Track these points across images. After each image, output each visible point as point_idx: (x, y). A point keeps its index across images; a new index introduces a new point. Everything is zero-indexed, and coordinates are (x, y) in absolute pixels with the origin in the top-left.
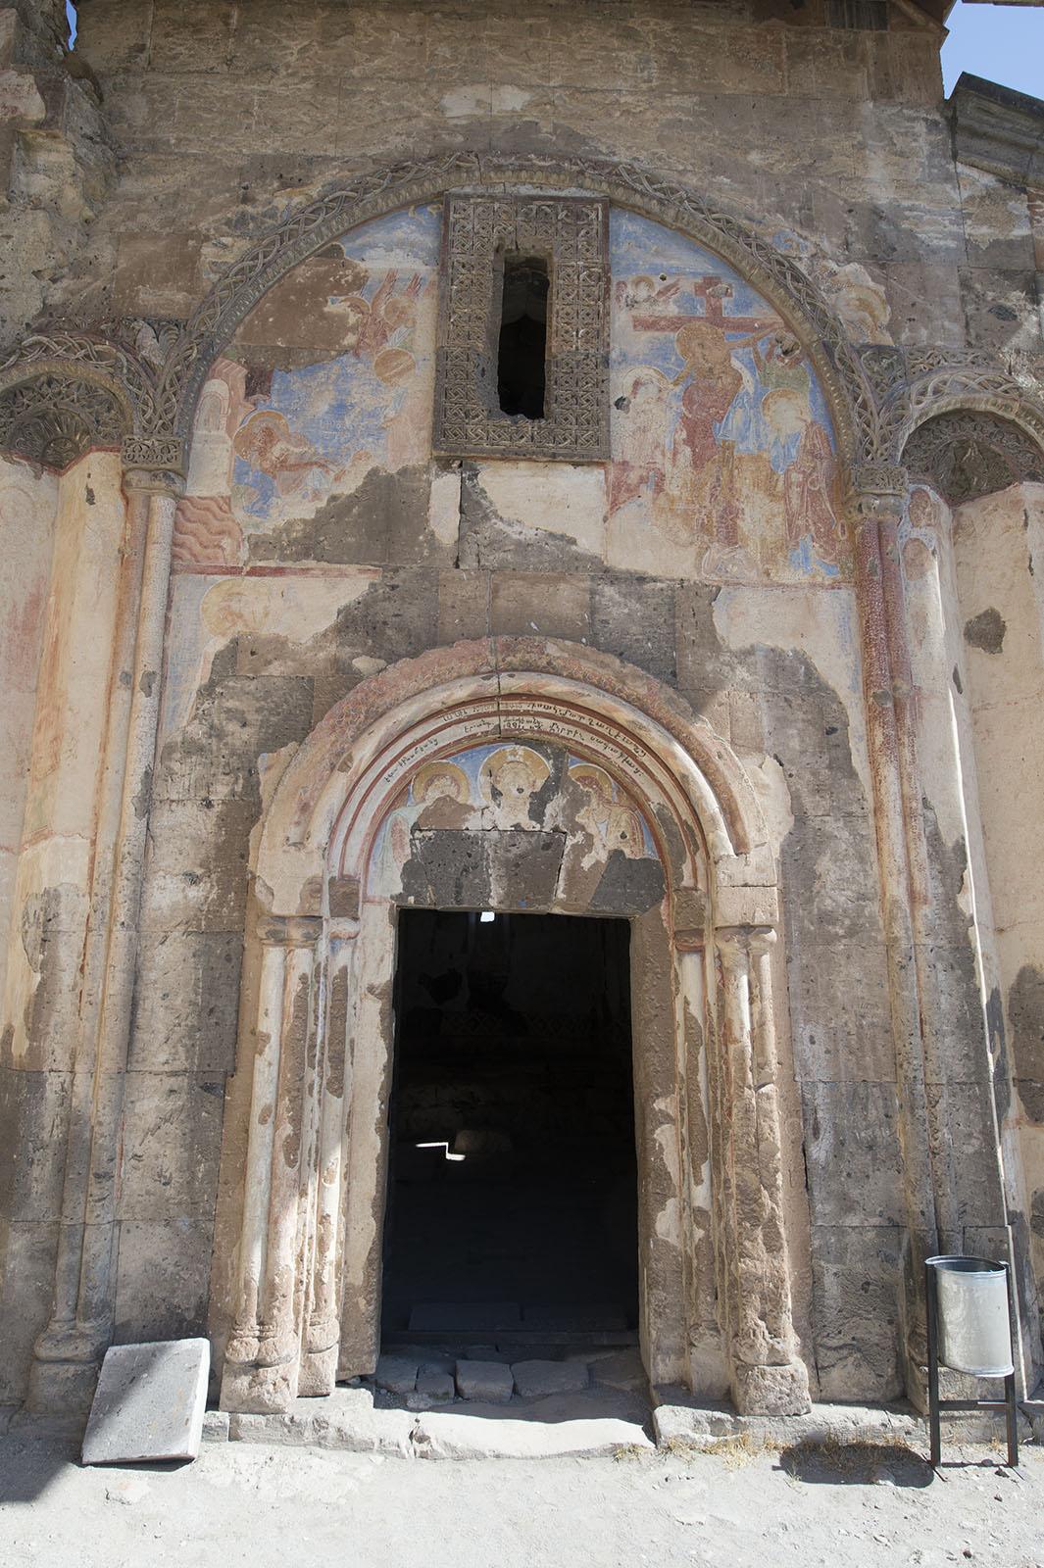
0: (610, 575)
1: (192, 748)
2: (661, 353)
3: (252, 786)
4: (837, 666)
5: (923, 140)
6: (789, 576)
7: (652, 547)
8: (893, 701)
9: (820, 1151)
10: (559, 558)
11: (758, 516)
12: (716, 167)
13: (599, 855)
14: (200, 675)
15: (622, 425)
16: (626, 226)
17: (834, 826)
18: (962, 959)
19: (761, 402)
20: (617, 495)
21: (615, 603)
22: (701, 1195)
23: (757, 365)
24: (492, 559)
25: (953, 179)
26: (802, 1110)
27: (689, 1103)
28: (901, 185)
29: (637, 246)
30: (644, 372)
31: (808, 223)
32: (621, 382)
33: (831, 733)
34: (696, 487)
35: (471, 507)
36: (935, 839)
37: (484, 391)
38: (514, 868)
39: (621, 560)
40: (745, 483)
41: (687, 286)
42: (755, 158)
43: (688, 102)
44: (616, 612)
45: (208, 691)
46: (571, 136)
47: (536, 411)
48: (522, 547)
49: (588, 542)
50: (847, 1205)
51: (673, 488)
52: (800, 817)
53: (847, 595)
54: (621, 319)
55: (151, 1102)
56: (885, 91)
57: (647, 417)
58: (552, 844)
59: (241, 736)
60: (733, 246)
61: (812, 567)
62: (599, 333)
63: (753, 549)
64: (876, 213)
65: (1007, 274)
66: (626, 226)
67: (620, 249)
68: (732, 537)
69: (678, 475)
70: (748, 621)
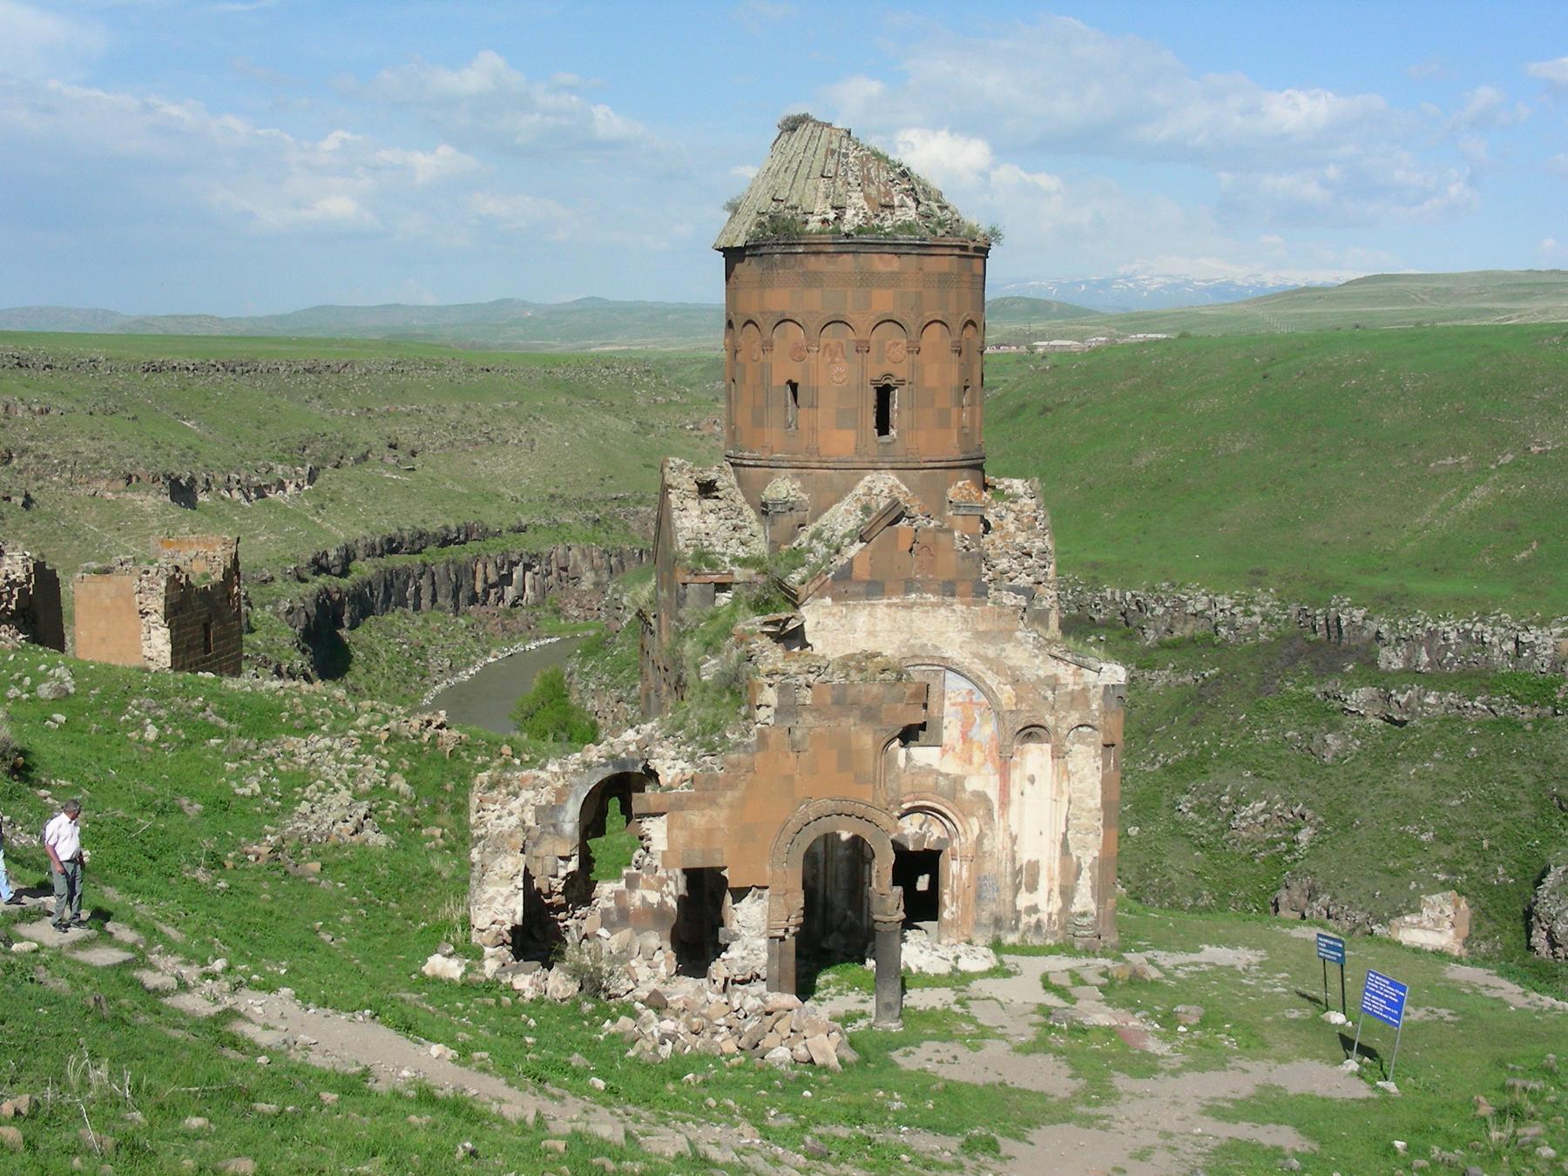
4: (993, 794)
6: (984, 771)
7: (951, 766)
10: (929, 770)
11: (977, 757)
15: (945, 733)
16: (949, 674)
18: (1014, 860)
19: (981, 726)
20: (944, 753)
21: (942, 781)
29: (952, 681)
33: (990, 811)
35: (908, 758)
38: (915, 842)
39: (943, 770)
46: (936, 648)
49: (936, 766)
53: (997, 777)
54: (947, 703)
55: (840, 895)
57: (951, 732)
58: (924, 836)
60: (977, 682)
62: (941, 709)
68: (971, 762)
69: (959, 746)
70: (973, 784)
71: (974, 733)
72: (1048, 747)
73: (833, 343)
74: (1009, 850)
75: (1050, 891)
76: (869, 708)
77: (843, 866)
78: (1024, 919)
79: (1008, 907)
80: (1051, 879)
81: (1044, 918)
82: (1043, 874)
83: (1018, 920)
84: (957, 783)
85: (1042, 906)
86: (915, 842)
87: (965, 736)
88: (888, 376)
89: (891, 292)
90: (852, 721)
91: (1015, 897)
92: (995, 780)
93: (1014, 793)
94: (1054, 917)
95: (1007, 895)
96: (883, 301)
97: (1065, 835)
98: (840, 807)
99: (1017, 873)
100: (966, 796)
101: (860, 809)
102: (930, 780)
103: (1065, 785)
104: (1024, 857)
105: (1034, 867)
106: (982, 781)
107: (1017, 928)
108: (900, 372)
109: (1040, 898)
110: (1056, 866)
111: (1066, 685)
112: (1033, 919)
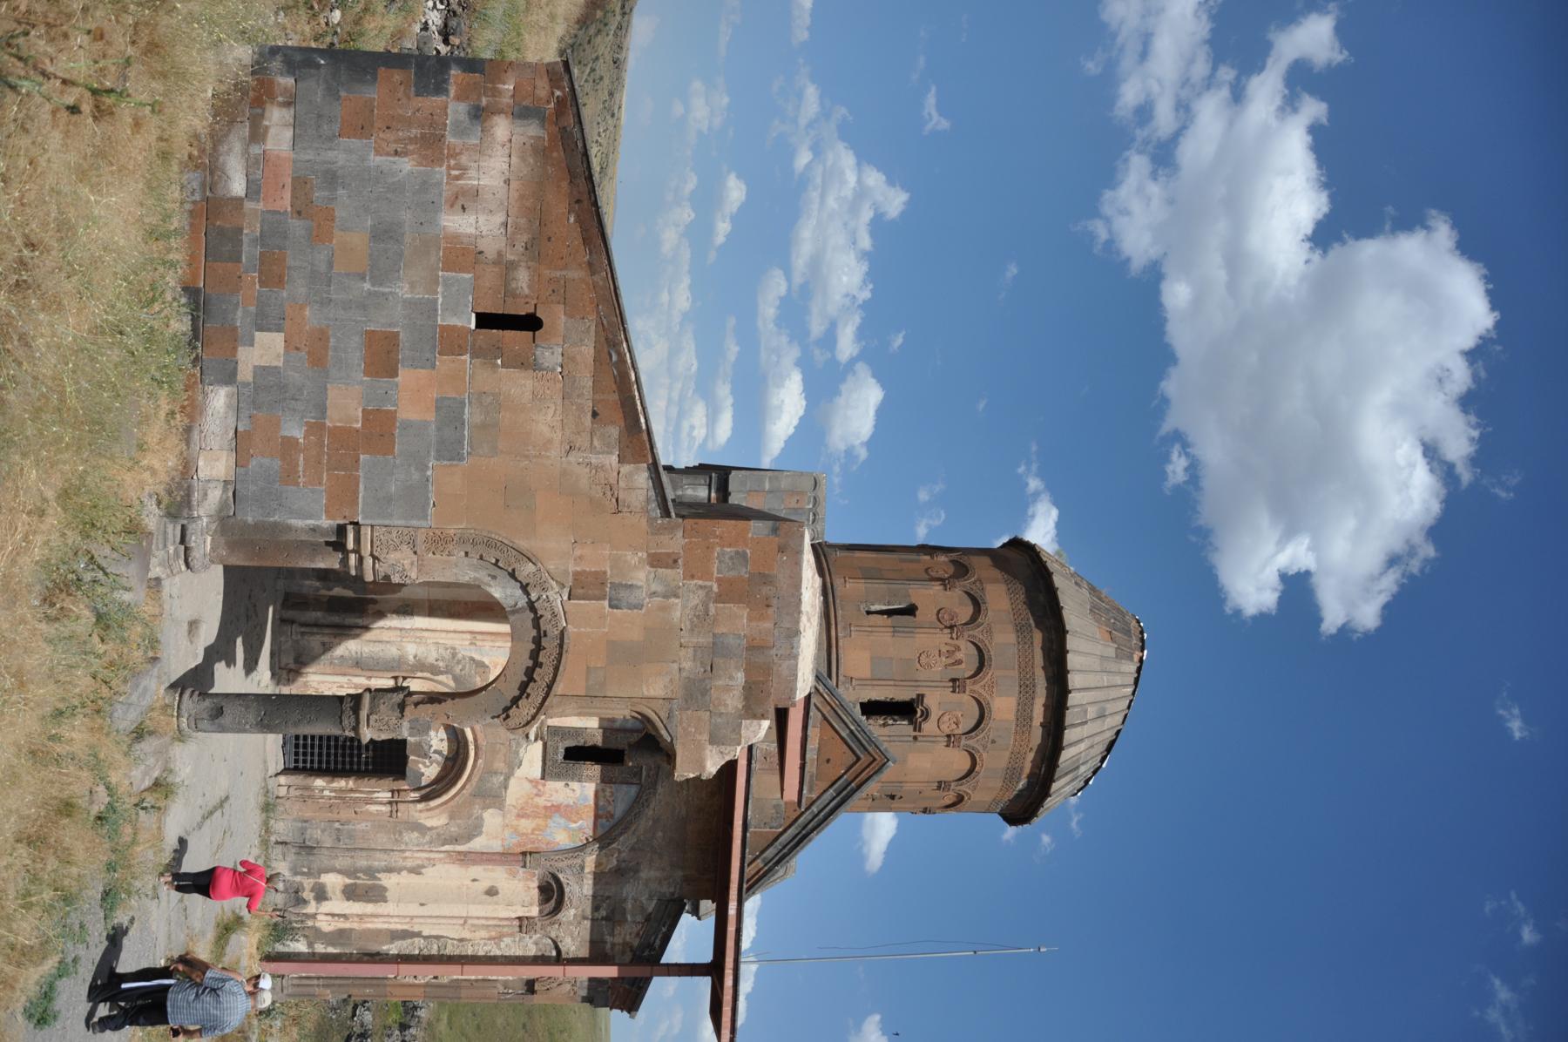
0: (507, 779)
1: (454, 655)
2: (586, 799)
3: (441, 673)
4: (477, 844)
5: (667, 890)
6: (507, 833)
7: (517, 790)
8: (466, 859)
9: (337, 825)
10: (513, 764)
11: (526, 825)
12: (656, 821)
13: (423, 770)
14: (477, 657)
15: (559, 785)
16: (633, 790)
17: (427, 838)
18: (389, 870)
19: (567, 829)
22: (327, 793)
23: (580, 829)
24: (514, 744)
25: (650, 898)
26: (348, 822)
27: (351, 790)
28: (648, 880)
30: (578, 792)
31: (632, 849)
32: (575, 785)
33: (455, 840)
34: (537, 807)
36: (423, 867)
37: (571, 743)
38: (419, 745)
39: (512, 782)
40: (540, 822)
41: (610, 808)
42: (660, 834)
43: (684, 812)
44: (495, 780)
45: (472, 659)
47: (566, 757)
48: (517, 753)
49: (518, 773)
50: (323, 831)
51: (537, 800)
52: (430, 829)
53: (500, 850)
56: (686, 879)
59: (457, 669)
61: (512, 842)
63: (515, 823)
64: (637, 871)
65: (613, 911)
66: (633, 790)
67: (624, 787)
68: (519, 816)
69: (541, 801)
70: (491, 819)
71: (558, 819)
72: (534, 911)
73: (959, 655)
74: (401, 863)
75: (345, 916)
76: (705, 692)
77: (393, 651)
78: (308, 883)
79: (326, 862)
80: (361, 917)
81: (311, 908)
82: (369, 908)
83: (308, 874)
84: (494, 798)
85: (326, 907)
86: (419, 745)
87: (555, 809)
88: (926, 715)
89: (1012, 717)
90: (687, 665)
91: (340, 872)
92: (496, 846)
93: (476, 871)
94: (310, 923)
95: (341, 862)
96: (1004, 706)
97: (419, 935)
98: (550, 644)
99: (371, 872)
100: (477, 810)
101: (543, 676)
102: (499, 765)
103: (484, 934)
104: (388, 880)
105: (375, 894)
106: (495, 831)
107: (296, 874)
108: (929, 727)
109: (337, 905)
110: (378, 924)
111: (612, 934)
112: (307, 895)
